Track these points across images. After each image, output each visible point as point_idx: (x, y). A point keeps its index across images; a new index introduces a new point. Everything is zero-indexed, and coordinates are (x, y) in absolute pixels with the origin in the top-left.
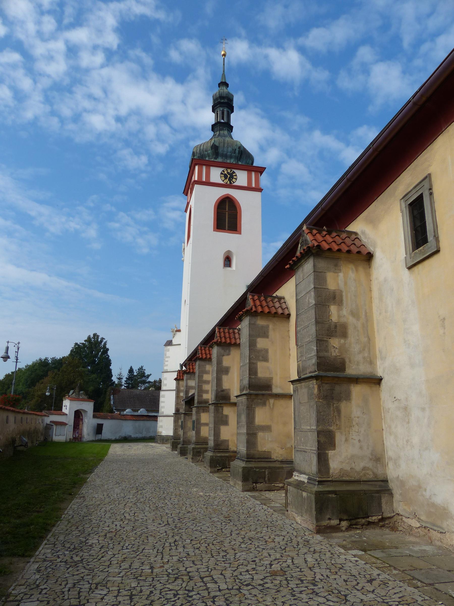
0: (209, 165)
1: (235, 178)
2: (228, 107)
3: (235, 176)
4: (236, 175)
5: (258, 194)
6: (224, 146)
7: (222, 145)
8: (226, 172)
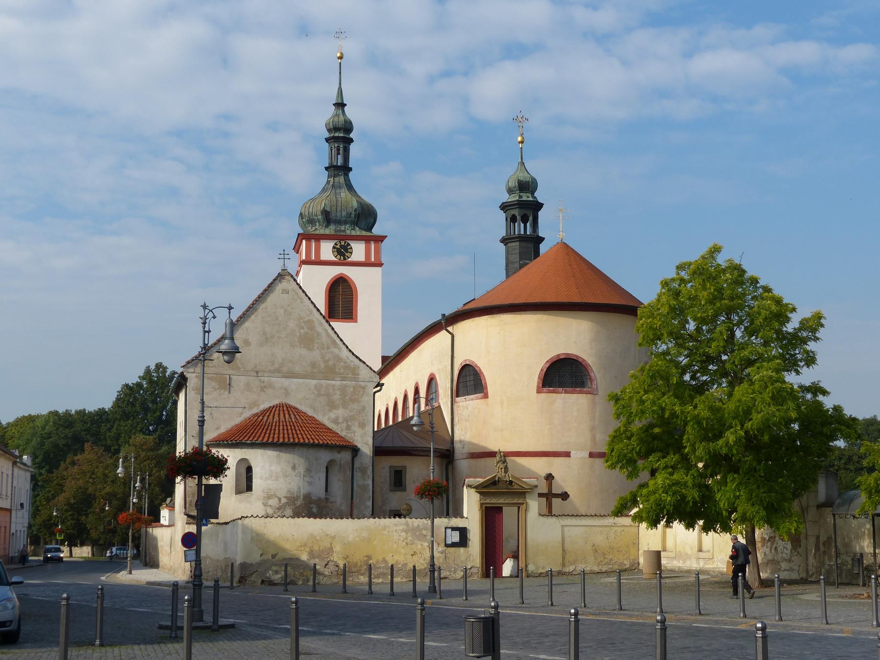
0: (319, 238)
1: (349, 252)
2: (344, 142)
3: (349, 249)
4: (351, 248)
5: (377, 270)
6: (337, 211)
7: (334, 209)
8: (338, 246)
